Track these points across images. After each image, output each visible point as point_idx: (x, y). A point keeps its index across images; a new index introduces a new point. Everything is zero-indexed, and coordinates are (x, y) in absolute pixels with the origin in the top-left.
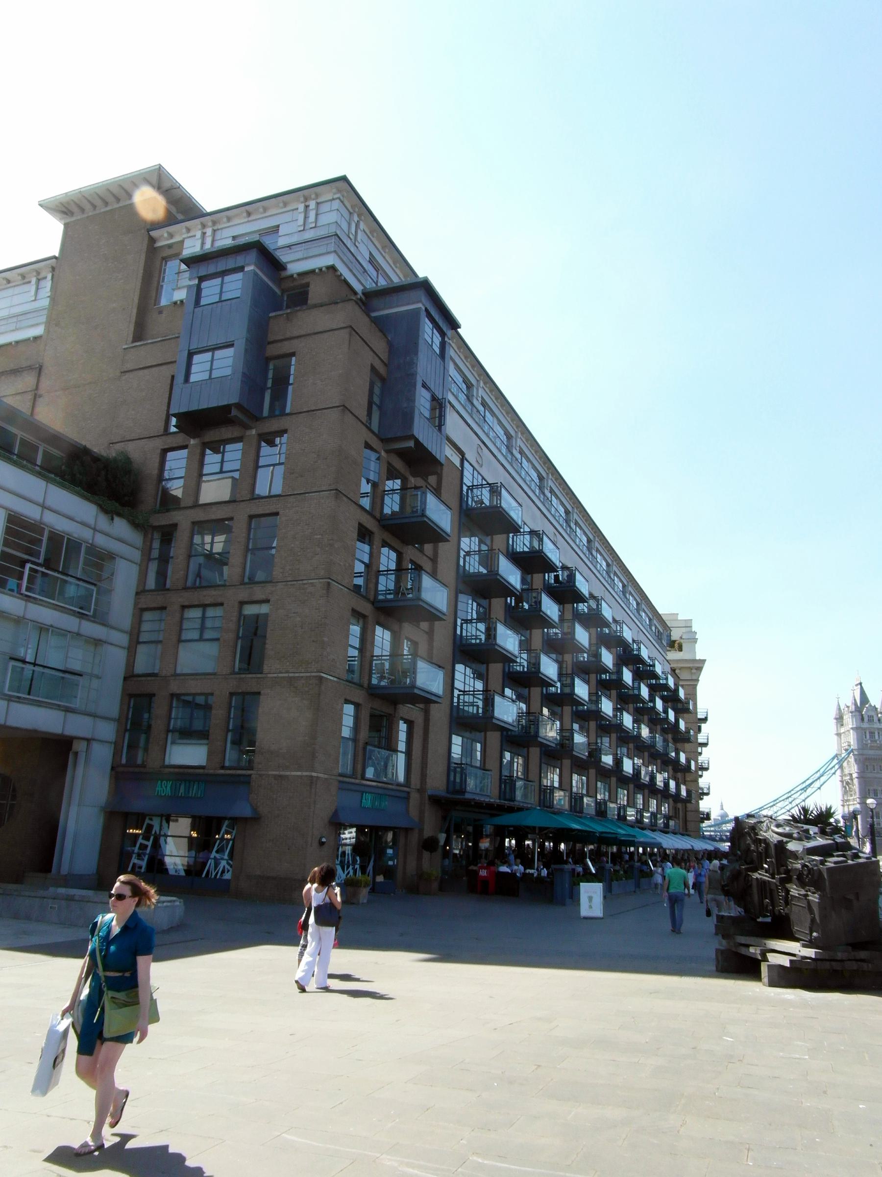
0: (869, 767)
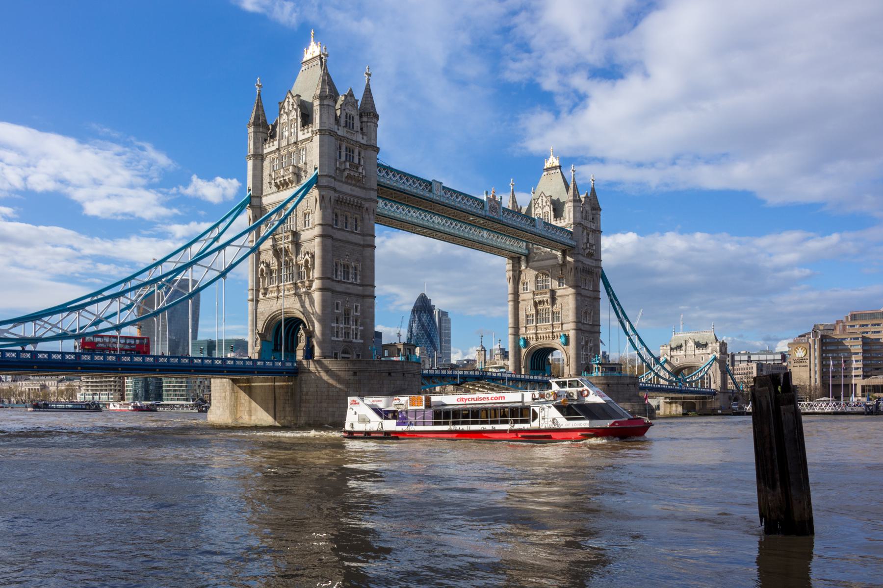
0: (340, 218)
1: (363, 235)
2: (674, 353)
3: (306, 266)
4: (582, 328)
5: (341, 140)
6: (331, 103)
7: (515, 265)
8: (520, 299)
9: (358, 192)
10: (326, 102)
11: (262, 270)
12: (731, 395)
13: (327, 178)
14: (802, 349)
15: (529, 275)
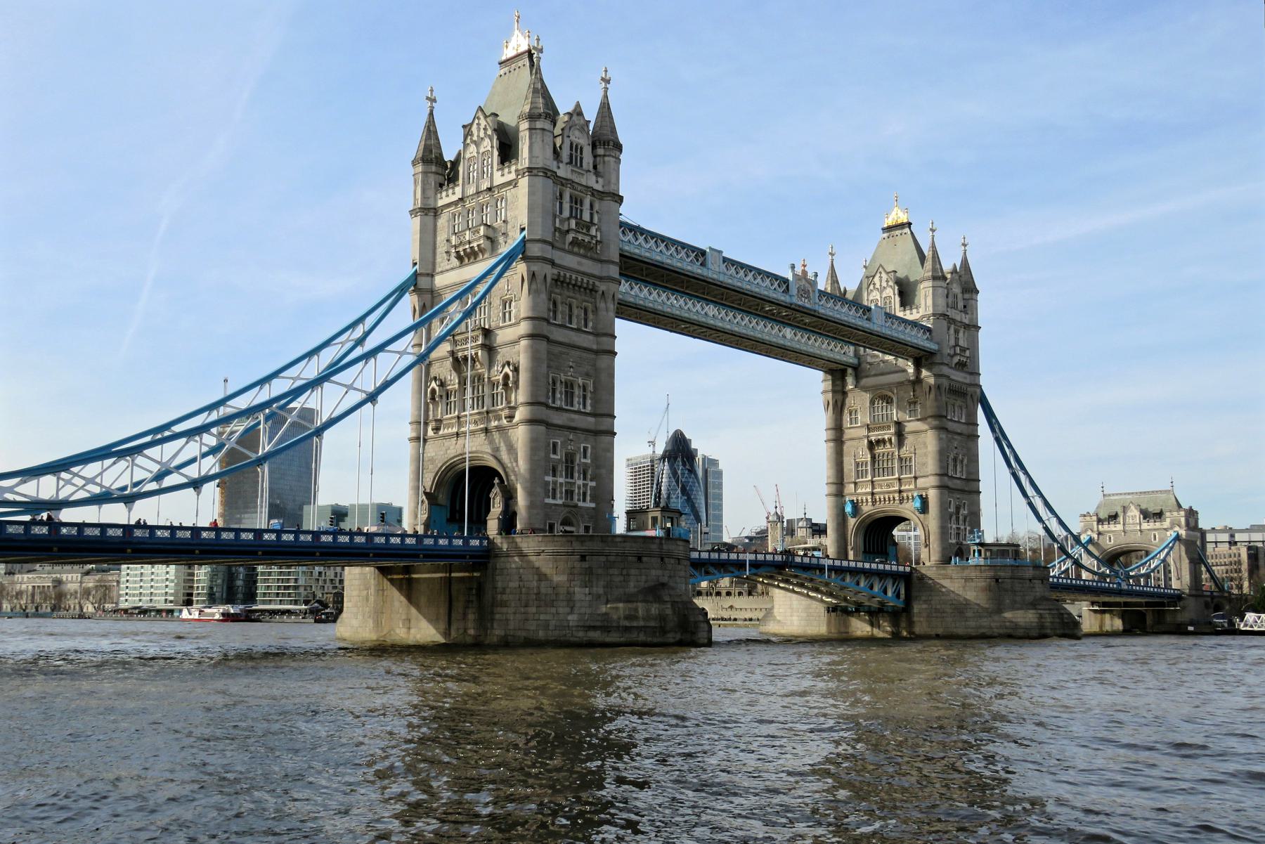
0: (560, 308)
3: (506, 385)
4: (950, 484)
5: (563, 185)
6: (548, 126)
7: (838, 383)
8: (846, 437)
9: (588, 266)
10: (539, 124)
11: (433, 391)
12: (1209, 599)
13: (539, 245)
15: (859, 400)
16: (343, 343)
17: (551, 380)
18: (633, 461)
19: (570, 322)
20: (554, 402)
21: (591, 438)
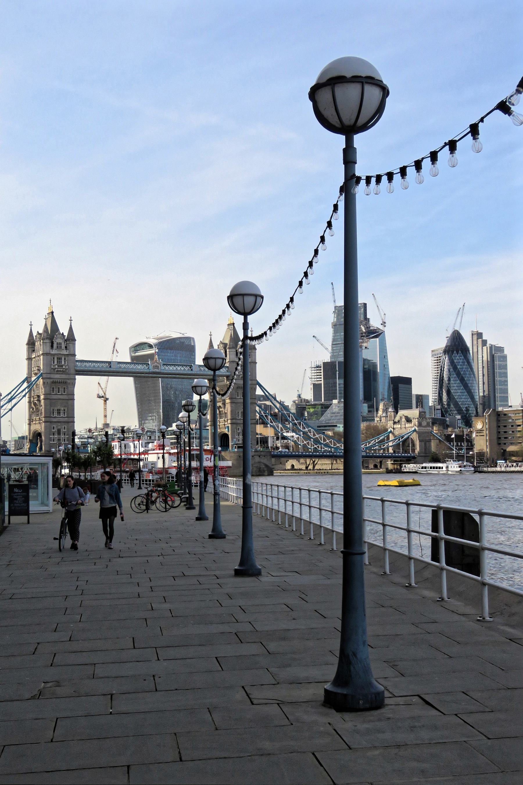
0: (55, 389)
1: (68, 395)
2: (395, 426)
9: (64, 376)
10: (45, 341)
14: (480, 423)
16: (5, 400)
17: (52, 410)
18: (436, 352)
19: (59, 393)
20: (53, 415)
21: (66, 424)
